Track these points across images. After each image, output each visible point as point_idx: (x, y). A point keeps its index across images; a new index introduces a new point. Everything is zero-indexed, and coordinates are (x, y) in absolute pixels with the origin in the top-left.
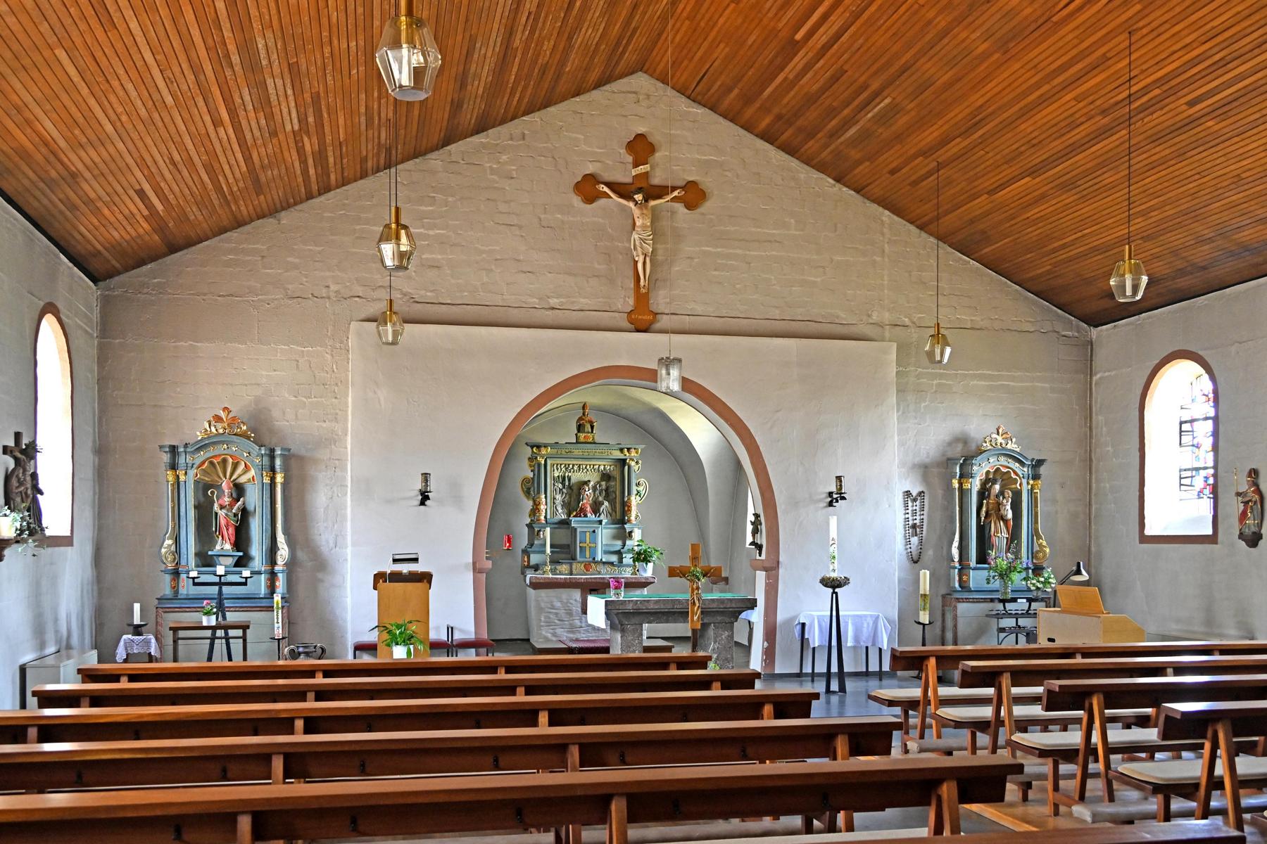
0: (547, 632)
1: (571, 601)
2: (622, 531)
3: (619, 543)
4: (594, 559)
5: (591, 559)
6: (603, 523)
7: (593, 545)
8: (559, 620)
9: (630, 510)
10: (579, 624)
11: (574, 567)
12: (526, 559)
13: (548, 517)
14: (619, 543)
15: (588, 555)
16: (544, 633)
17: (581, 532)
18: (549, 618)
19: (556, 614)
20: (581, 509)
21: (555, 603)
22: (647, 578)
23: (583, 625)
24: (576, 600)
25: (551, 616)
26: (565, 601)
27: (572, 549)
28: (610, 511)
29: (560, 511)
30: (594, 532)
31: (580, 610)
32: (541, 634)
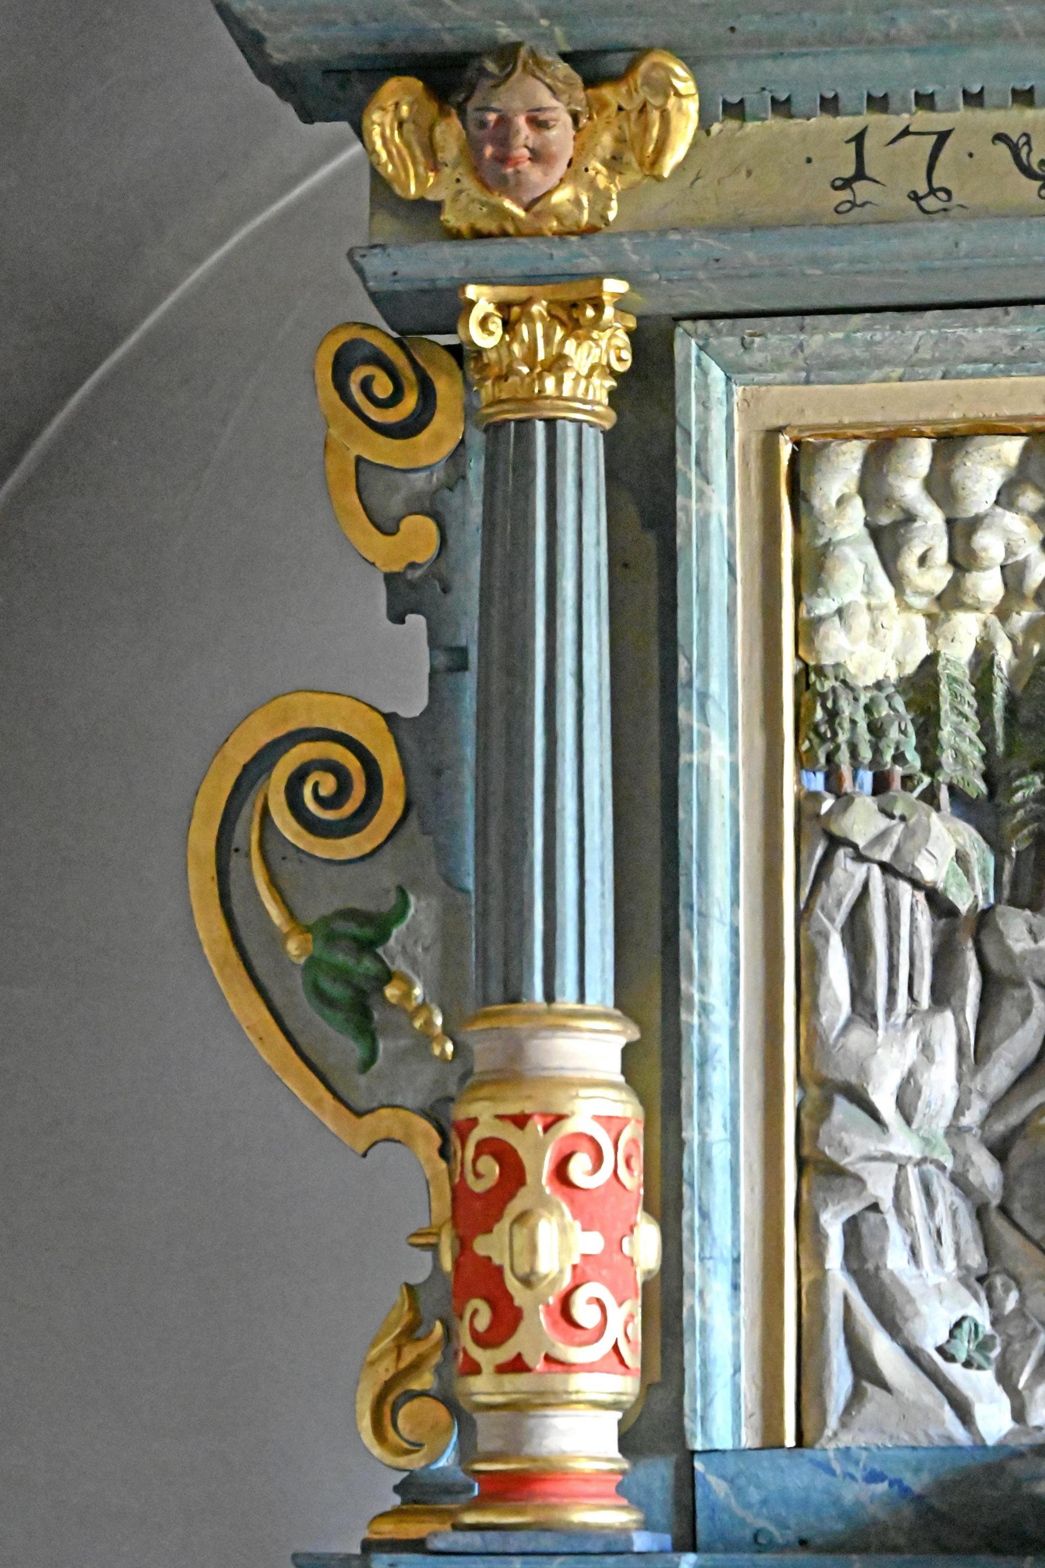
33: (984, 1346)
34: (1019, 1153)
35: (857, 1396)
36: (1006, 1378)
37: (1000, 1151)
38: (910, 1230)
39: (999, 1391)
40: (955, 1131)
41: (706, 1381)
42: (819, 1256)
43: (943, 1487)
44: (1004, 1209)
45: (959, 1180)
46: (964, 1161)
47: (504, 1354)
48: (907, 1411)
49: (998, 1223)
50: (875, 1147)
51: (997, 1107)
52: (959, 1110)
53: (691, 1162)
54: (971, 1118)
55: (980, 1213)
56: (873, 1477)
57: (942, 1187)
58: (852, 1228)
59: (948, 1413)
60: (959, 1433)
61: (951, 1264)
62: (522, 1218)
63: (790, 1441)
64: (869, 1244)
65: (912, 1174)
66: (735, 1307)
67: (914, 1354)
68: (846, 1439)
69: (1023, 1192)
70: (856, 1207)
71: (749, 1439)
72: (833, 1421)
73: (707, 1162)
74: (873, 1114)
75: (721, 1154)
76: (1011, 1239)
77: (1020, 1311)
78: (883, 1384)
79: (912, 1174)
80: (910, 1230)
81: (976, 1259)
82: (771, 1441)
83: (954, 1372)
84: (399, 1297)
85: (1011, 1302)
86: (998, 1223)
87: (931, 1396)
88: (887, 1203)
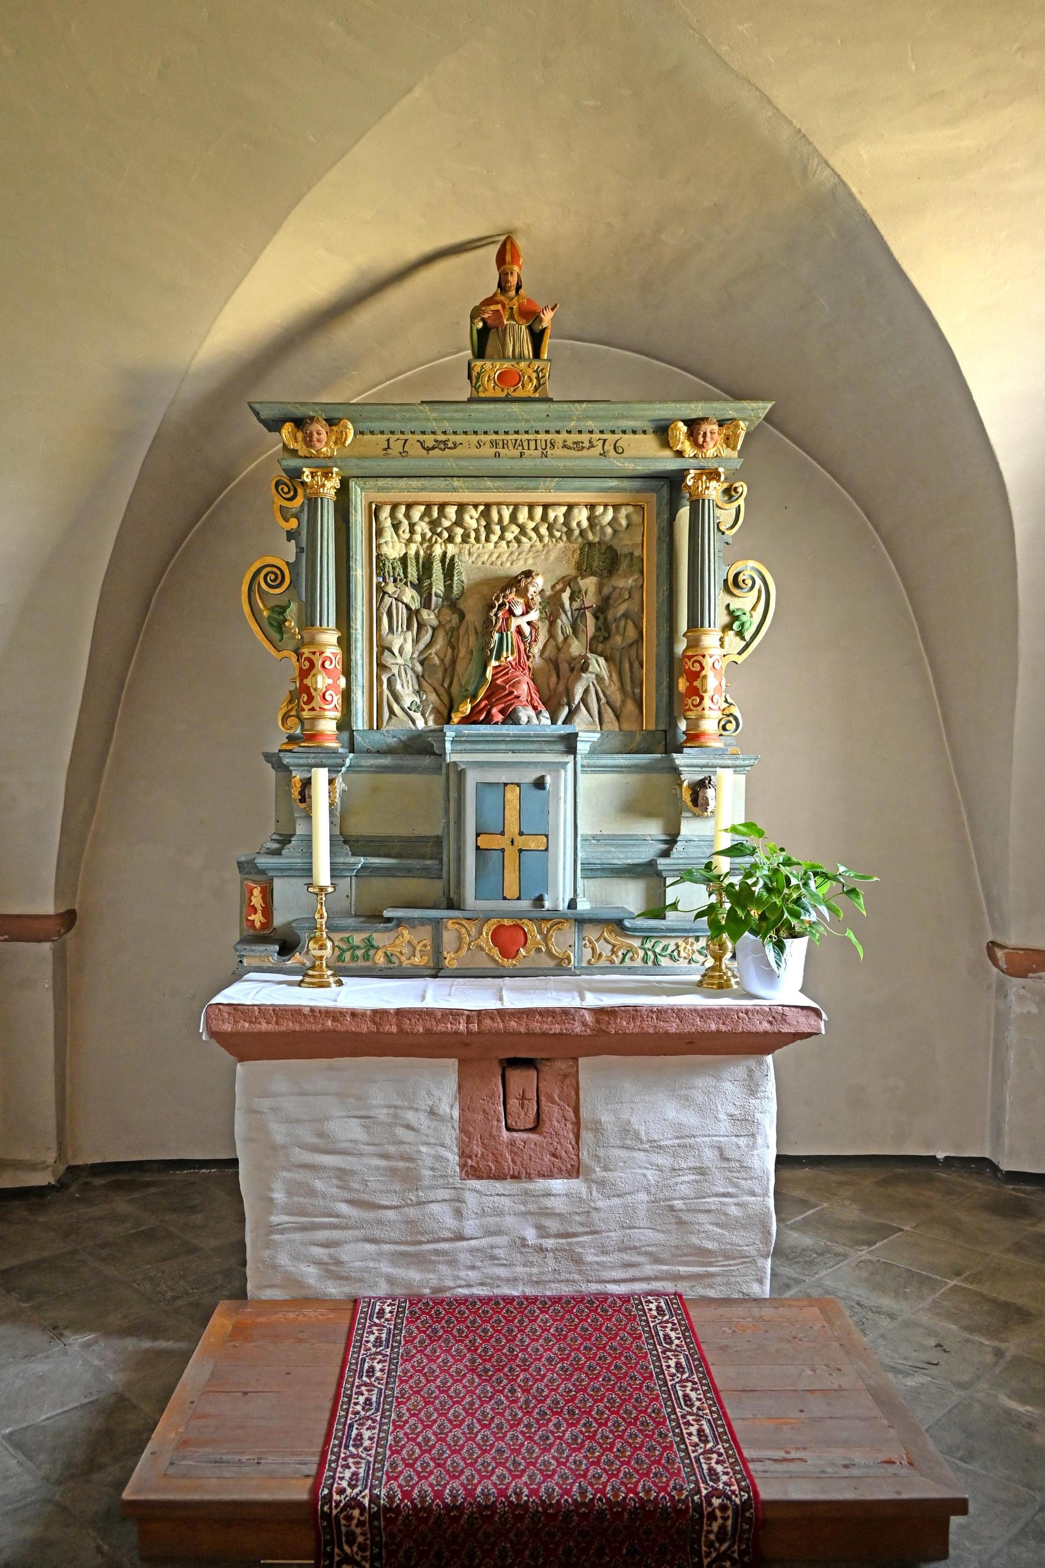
0: (296, 1258)
1: (410, 1116)
2: (663, 779)
3: (653, 829)
4: (539, 901)
5: (525, 904)
6: (582, 747)
7: (533, 843)
8: (351, 1202)
9: (696, 692)
10: (450, 1222)
11: (448, 937)
12: (257, 900)
13: (360, 722)
14: (653, 829)
15: (511, 888)
16: (283, 1259)
17: (482, 786)
18: (312, 1193)
19: (342, 1174)
20: (494, 690)
21: (333, 1127)
22: (776, 1015)
23: (470, 1226)
24: (432, 1113)
25: (319, 1185)
26: (382, 1114)
27: (449, 853)
28: (617, 697)
29: (408, 697)
30: (539, 784)
31: (453, 1158)
32: (274, 1267)
33: (418, 707)
34: (426, 663)
35: (390, 718)
36: (423, 714)
37: (422, 663)
38: (402, 680)
39: (422, 718)
40: (412, 658)
41: (356, 714)
42: (382, 686)
43: (410, 739)
44: (422, 676)
45: (413, 669)
46: (414, 665)
47: (310, 707)
48: (401, 721)
49: (422, 679)
50: (393, 661)
51: (421, 653)
52: (413, 654)
53: (353, 664)
54: (415, 655)
55: (418, 677)
56: (394, 737)
57: (409, 672)
58: (389, 680)
59: (410, 722)
60: (413, 727)
61: (411, 688)
62: (314, 675)
63: (375, 728)
64: (393, 684)
65: (402, 667)
66: (363, 697)
67: (403, 709)
68: (387, 728)
69: (426, 673)
70: (390, 675)
71: (366, 727)
72: (385, 724)
73: (356, 664)
74: (393, 654)
75: (360, 662)
76: (424, 683)
77: (426, 699)
78: (396, 715)
79: (402, 667)
80: (402, 680)
81: (417, 687)
82: (371, 728)
83: (412, 713)
84: (288, 693)
85: (424, 697)
86: (422, 679)
87: (406, 718)
88: (397, 674)
